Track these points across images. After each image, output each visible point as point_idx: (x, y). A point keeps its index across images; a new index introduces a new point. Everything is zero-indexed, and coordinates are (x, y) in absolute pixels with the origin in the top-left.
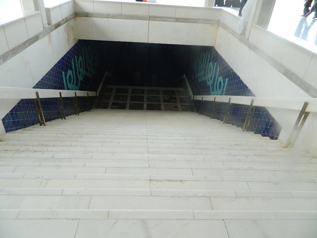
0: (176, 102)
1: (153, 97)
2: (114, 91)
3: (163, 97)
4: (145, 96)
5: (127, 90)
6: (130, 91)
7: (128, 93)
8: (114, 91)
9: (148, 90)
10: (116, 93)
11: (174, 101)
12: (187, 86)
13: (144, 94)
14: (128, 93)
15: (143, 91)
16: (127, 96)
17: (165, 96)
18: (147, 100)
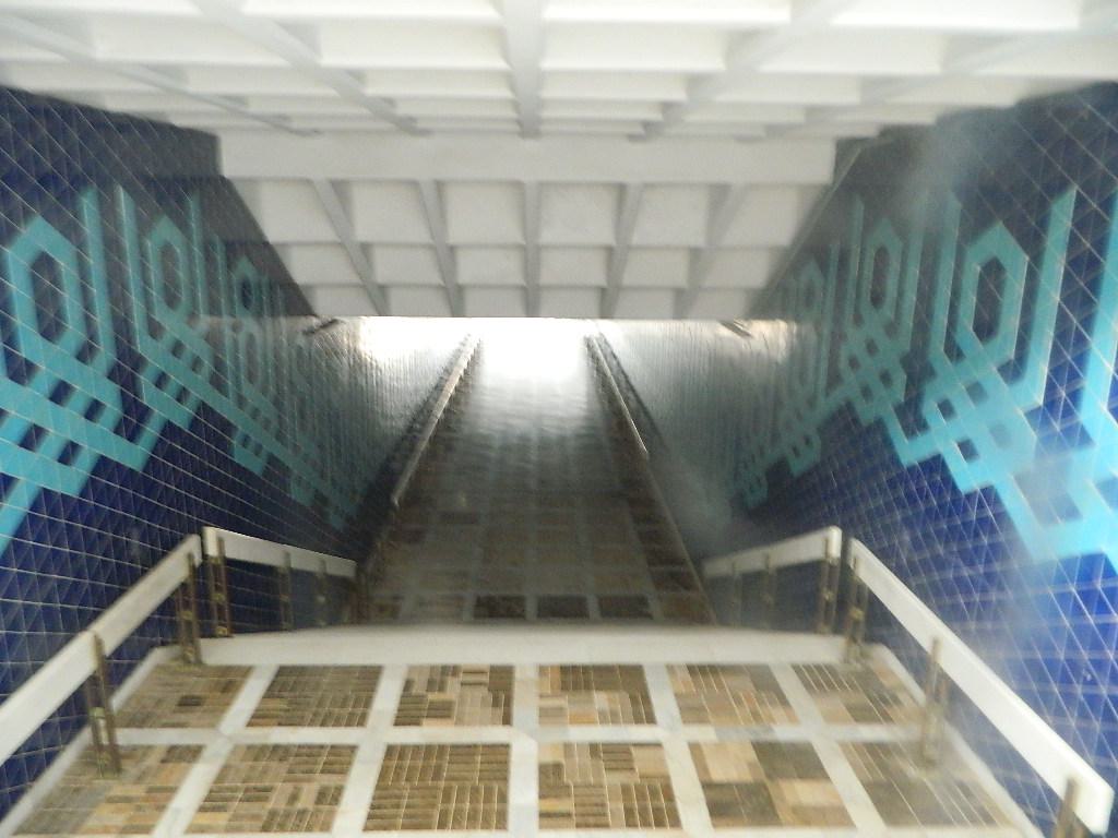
0: (837, 816)
1: (594, 749)
2: (249, 697)
3: (695, 749)
4: (527, 749)
5: (369, 677)
6: (387, 698)
7: (362, 721)
8: (249, 697)
9: (542, 670)
10: (258, 718)
11: (802, 792)
12: (926, 644)
13: (507, 720)
14: (362, 721)
15: (499, 685)
16: (340, 759)
17: (705, 734)
18: (542, 796)
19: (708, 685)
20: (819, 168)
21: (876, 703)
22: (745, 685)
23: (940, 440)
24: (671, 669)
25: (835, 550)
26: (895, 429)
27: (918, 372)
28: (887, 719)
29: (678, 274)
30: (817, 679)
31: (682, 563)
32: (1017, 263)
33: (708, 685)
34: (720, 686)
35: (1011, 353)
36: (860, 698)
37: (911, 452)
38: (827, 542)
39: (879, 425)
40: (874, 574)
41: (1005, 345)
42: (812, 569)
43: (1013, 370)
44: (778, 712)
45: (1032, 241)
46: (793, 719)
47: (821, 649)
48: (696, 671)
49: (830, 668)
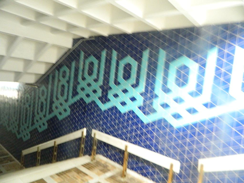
19: (66, 178)
20: (68, 44)
21: (105, 169)
22: (75, 174)
23: (114, 102)
24: (52, 177)
25: (85, 134)
26: (99, 103)
27: (105, 89)
28: (109, 170)
29: (19, 67)
30: (87, 166)
31: (7, 154)
32: (134, 64)
33: (66, 178)
34: (69, 176)
35: (134, 82)
36: (101, 168)
37: (104, 107)
38: (83, 133)
39: (94, 102)
40: (100, 136)
41: (133, 80)
42: (79, 139)
43: (135, 86)
44: (87, 177)
45: (139, 60)
46: (91, 178)
47: (84, 159)
48: (59, 174)
49: (89, 163)
